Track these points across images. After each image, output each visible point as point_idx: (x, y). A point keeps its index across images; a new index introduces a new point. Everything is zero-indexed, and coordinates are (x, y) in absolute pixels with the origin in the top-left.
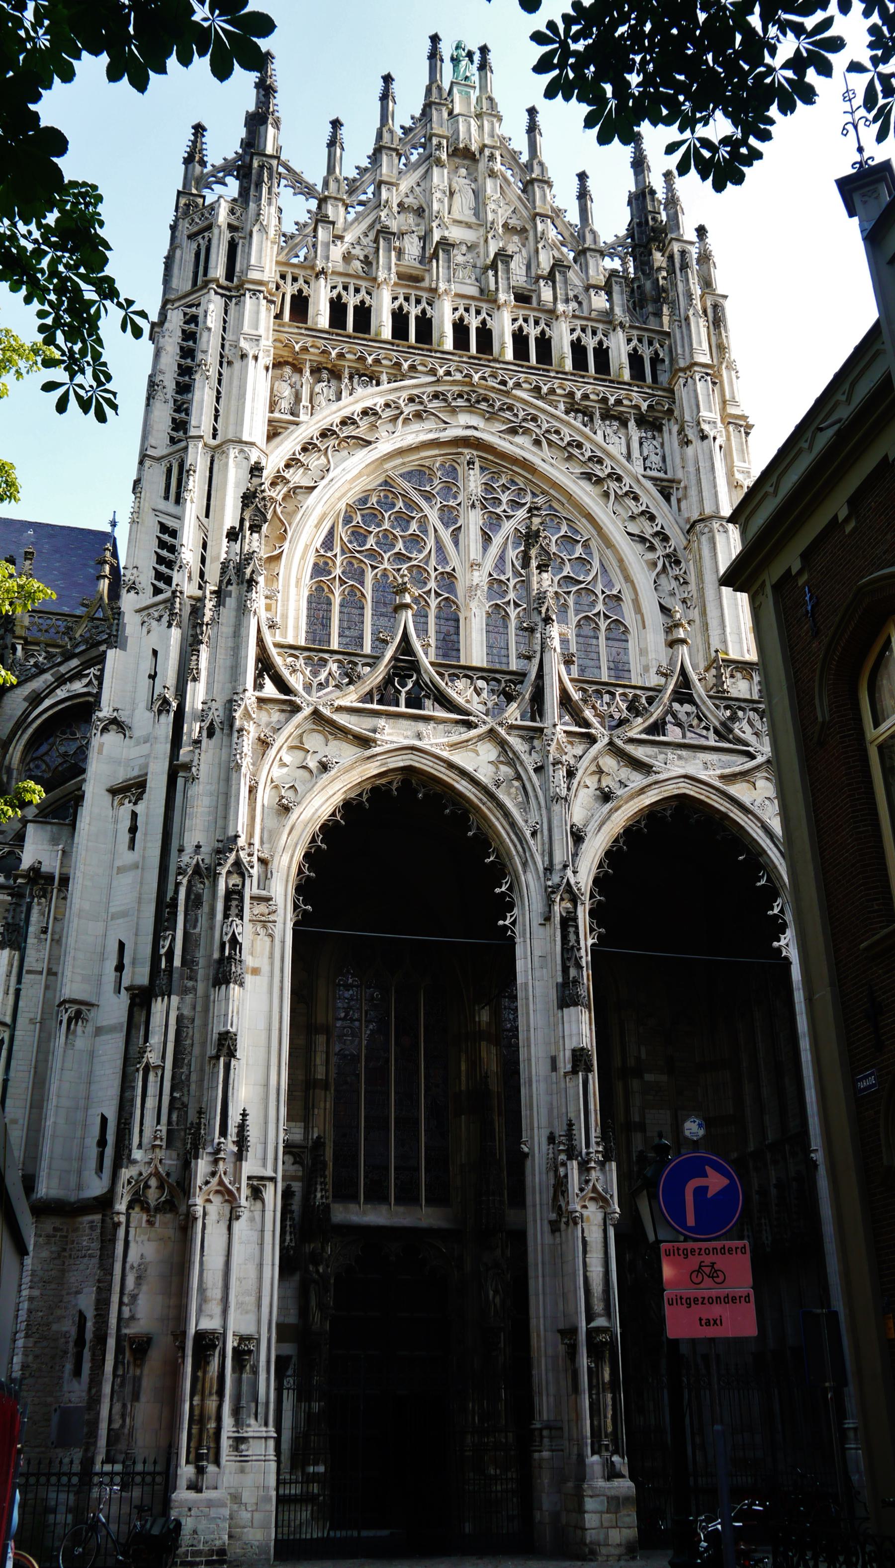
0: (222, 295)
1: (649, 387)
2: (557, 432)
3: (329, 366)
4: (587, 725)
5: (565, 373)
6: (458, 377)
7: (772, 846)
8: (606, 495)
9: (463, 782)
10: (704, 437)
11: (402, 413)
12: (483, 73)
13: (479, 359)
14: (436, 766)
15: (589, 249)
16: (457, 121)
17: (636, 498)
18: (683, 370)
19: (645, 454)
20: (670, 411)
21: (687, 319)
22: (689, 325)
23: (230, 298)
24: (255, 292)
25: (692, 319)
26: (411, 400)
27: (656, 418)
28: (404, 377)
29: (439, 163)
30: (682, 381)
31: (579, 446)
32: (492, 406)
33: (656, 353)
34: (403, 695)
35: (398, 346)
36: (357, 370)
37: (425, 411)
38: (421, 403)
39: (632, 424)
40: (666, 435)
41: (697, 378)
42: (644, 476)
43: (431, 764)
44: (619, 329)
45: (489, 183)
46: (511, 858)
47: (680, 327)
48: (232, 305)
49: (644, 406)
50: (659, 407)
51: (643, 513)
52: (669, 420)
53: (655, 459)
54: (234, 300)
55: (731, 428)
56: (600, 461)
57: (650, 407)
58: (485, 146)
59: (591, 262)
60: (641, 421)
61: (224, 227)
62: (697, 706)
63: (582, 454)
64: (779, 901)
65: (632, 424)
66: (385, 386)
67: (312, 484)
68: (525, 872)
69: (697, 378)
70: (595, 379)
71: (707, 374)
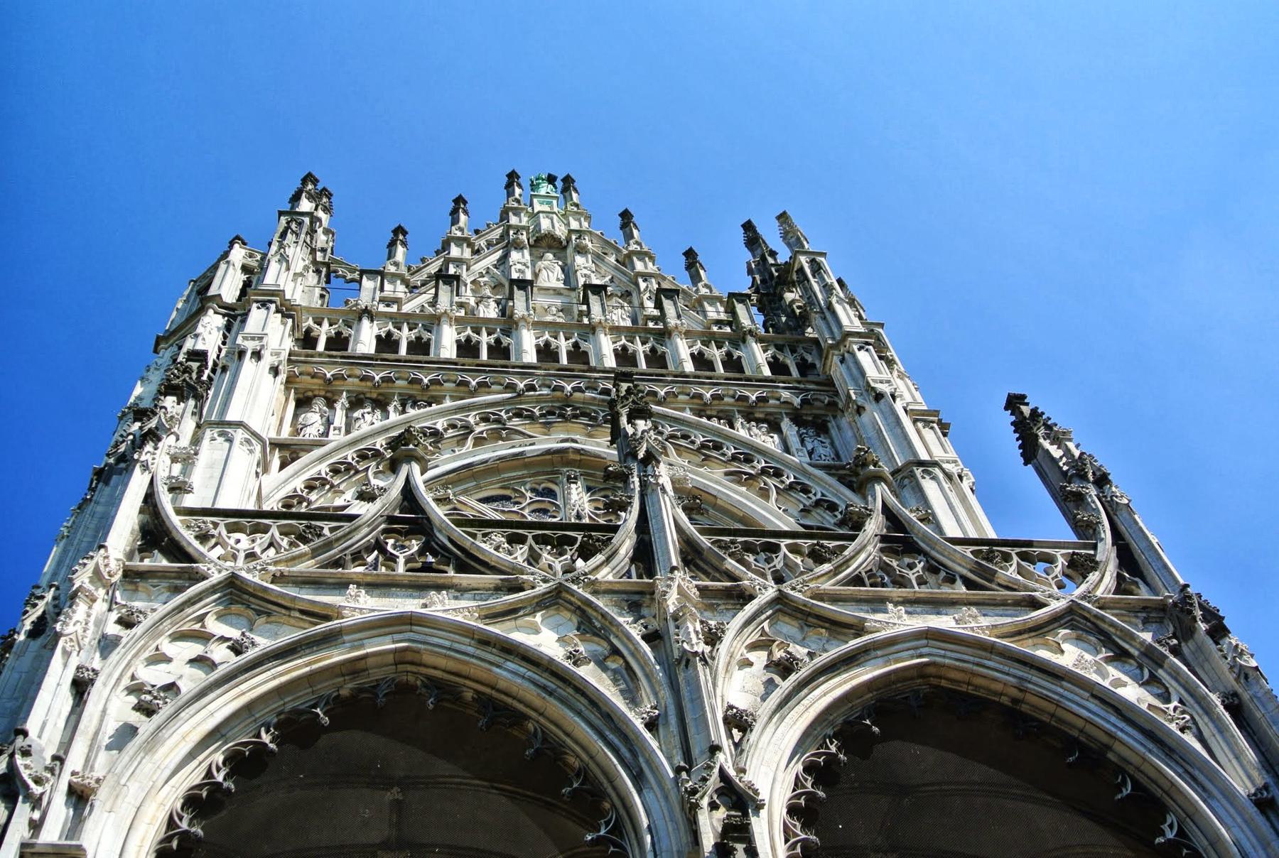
0: (224, 315)
1: (799, 382)
2: (685, 437)
3: (374, 396)
4: (732, 577)
5: (687, 376)
6: (545, 391)
7: (1122, 725)
8: (764, 493)
9: (510, 665)
10: (879, 397)
11: (472, 431)
12: (567, 194)
13: (572, 370)
14: (456, 646)
15: (705, 298)
16: (539, 217)
17: (806, 490)
18: (836, 346)
19: (810, 447)
20: (833, 405)
21: (830, 307)
22: (834, 313)
23: (234, 318)
24: (264, 304)
25: (839, 309)
26: (485, 419)
27: (816, 416)
28: (473, 394)
29: (519, 247)
30: (836, 359)
31: (717, 447)
32: (595, 419)
33: (803, 359)
34: (401, 561)
35: (463, 365)
36: (411, 397)
37: (504, 429)
38: (498, 421)
39: (786, 424)
40: (834, 432)
41: (855, 347)
42: (810, 464)
43: (447, 643)
44: (749, 337)
45: (579, 260)
46: (612, 779)
47: (824, 318)
48: (236, 324)
49: (797, 401)
50: (817, 404)
51: (818, 503)
52: (835, 417)
53: (824, 452)
54: (239, 318)
55: (920, 425)
56: (748, 460)
57: (804, 402)
58: (571, 231)
59: (708, 307)
60: (797, 419)
61: (238, 266)
62: (926, 554)
63: (724, 455)
64: (1170, 818)
65: (786, 424)
66: (448, 403)
67: (346, 504)
68: (640, 792)
69: (855, 347)
70: (727, 379)
71: (867, 344)
